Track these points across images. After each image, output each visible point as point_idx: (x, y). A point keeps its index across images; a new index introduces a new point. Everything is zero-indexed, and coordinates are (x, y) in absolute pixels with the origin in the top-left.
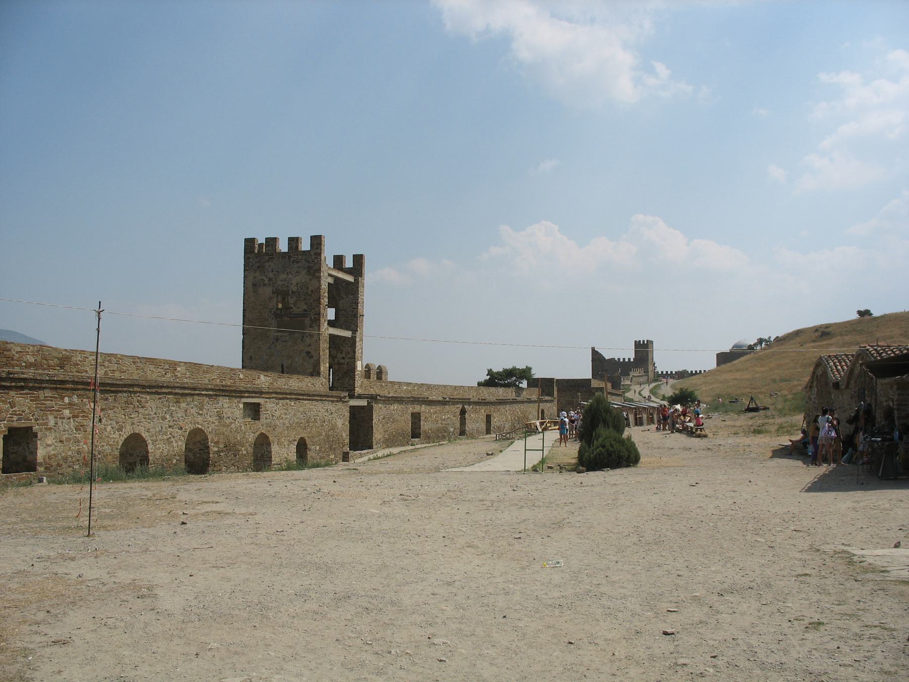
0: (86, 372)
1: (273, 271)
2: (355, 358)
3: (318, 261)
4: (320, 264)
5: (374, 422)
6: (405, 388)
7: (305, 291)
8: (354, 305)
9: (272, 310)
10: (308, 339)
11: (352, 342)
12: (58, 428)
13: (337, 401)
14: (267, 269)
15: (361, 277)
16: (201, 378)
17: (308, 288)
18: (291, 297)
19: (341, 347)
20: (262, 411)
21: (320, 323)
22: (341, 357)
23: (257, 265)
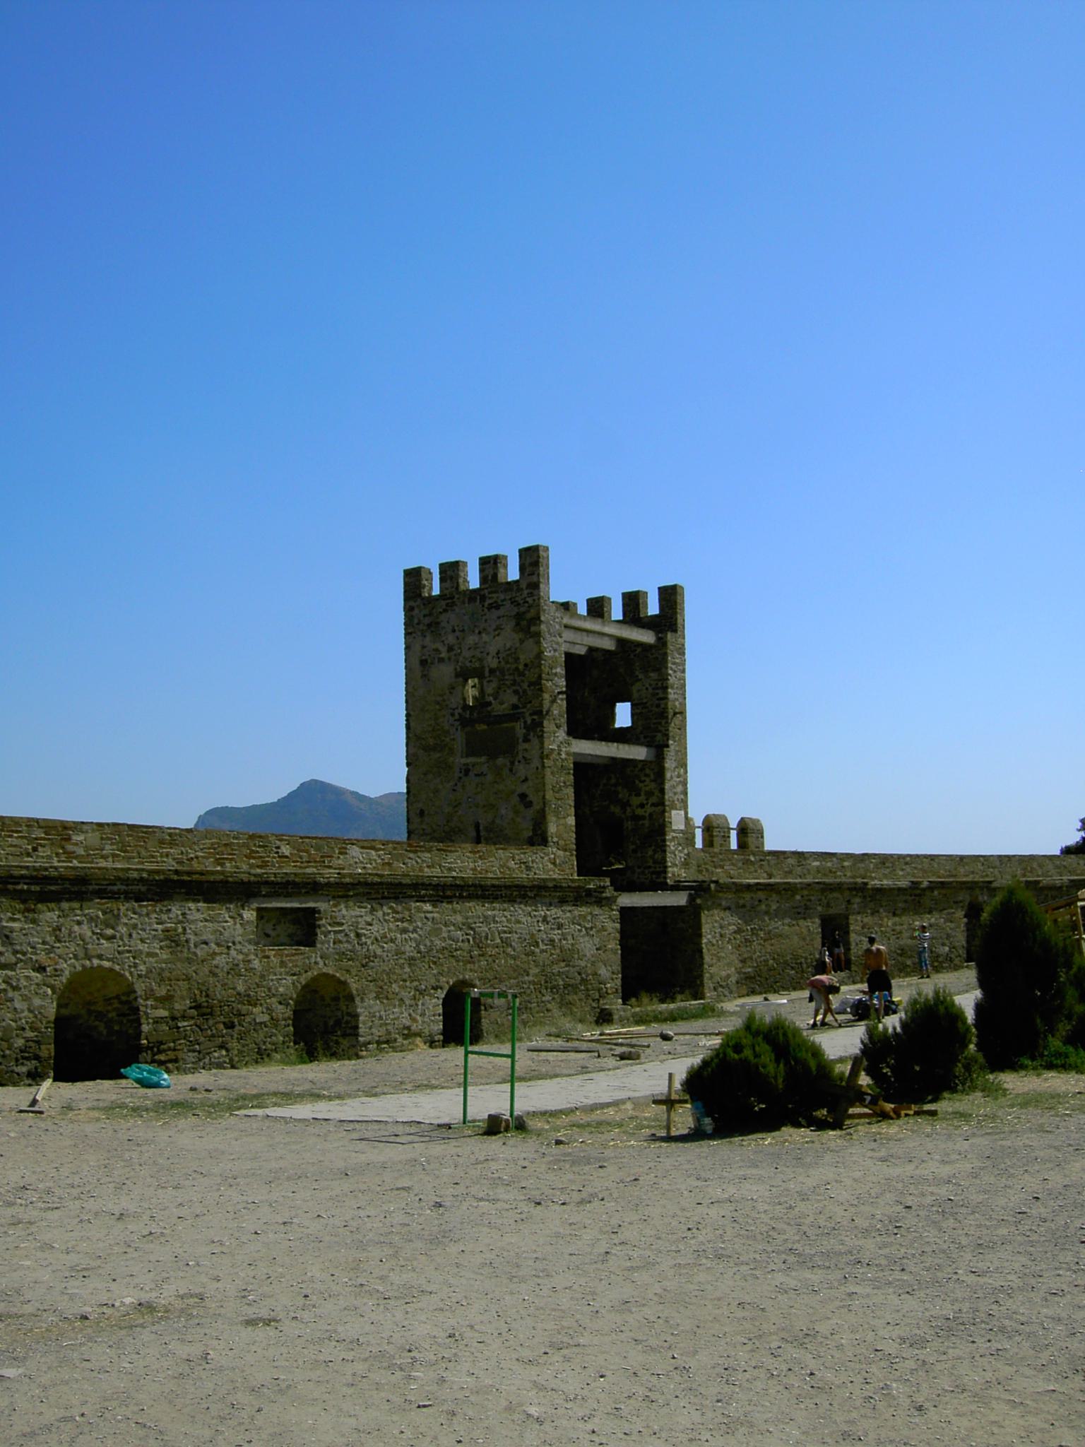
3: (534, 600)
4: (539, 605)
5: (704, 941)
6: (817, 863)
7: (514, 666)
8: (660, 691)
9: (456, 712)
10: (521, 767)
11: (656, 769)
14: (444, 628)
15: (675, 631)
17: (517, 659)
18: (489, 682)
19: (637, 782)
20: (319, 927)
21: (543, 731)
22: (638, 803)
23: (427, 620)
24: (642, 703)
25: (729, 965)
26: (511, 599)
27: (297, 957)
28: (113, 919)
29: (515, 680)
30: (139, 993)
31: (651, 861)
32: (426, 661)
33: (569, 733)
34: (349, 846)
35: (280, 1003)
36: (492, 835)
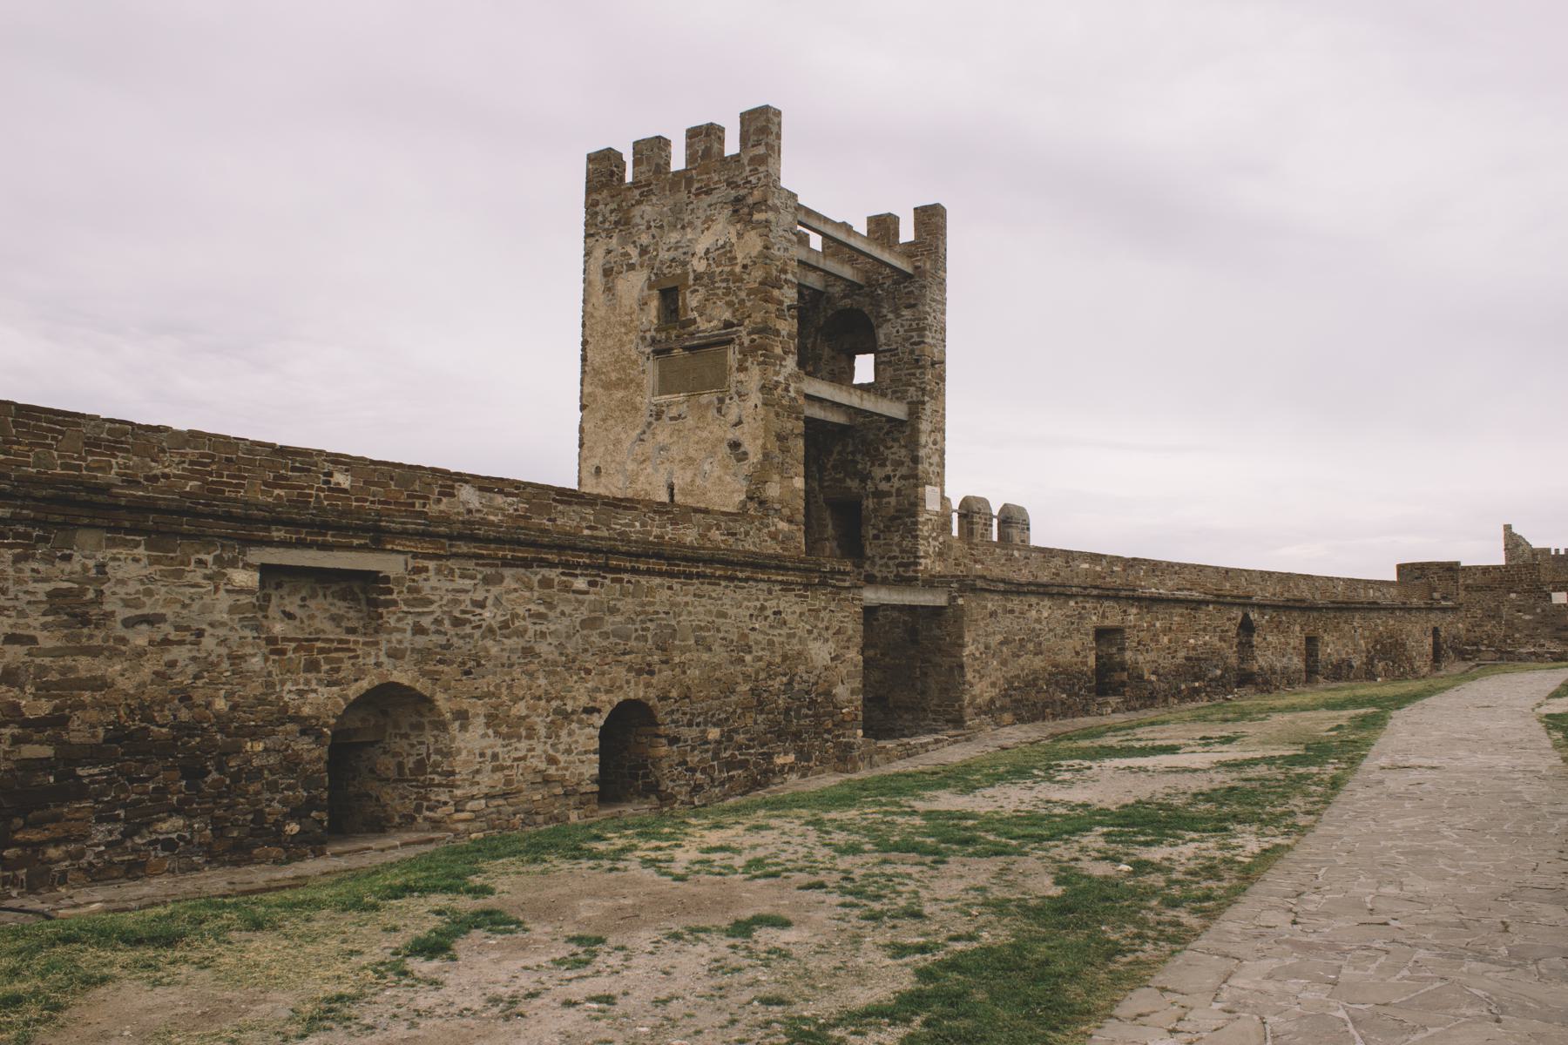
1: (649, 227)
6: (1086, 566)
7: (727, 269)
8: (914, 334)
13: (806, 586)
19: (882, 449)
23: (613, 218)
26: (726, 180)
27: (341, 655)
29: (728, 288)
31: (897, 550)
33: (800, 364)
34: (457, 485)
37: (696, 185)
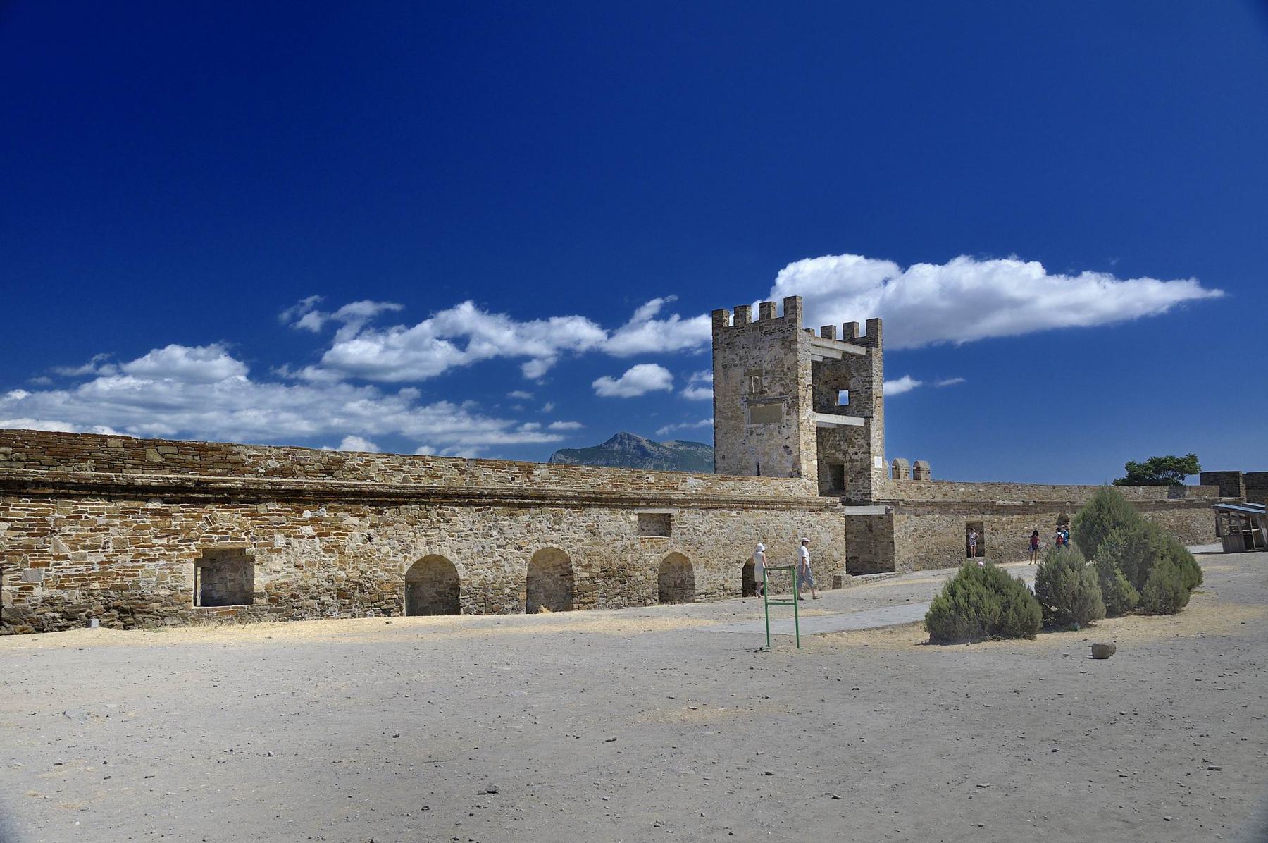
0: (371, 478)
2: (870, 453)
6: (963, 489)
9: (745, 396)
10: (785, 430)
12: (293, 550)
16: (578, 483)
19: (853, 439)
23: (727, 341)
24: (856, 391)
25: (909, 551)
28: (558, 521)
30: (573, 563)
32: (726, 366)
33: (814, 409)
35: (651, 569)
36: (766, 470)
37: (765, 330)
